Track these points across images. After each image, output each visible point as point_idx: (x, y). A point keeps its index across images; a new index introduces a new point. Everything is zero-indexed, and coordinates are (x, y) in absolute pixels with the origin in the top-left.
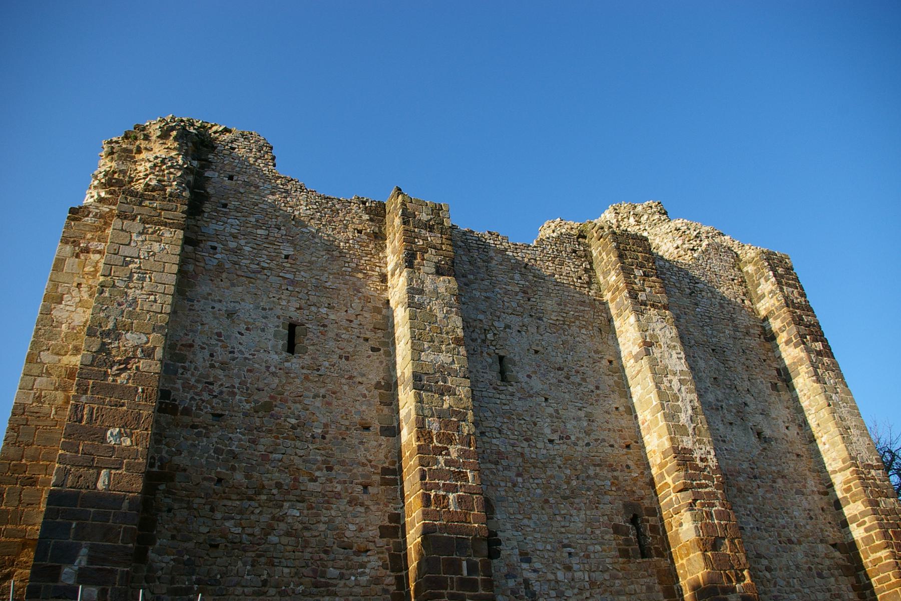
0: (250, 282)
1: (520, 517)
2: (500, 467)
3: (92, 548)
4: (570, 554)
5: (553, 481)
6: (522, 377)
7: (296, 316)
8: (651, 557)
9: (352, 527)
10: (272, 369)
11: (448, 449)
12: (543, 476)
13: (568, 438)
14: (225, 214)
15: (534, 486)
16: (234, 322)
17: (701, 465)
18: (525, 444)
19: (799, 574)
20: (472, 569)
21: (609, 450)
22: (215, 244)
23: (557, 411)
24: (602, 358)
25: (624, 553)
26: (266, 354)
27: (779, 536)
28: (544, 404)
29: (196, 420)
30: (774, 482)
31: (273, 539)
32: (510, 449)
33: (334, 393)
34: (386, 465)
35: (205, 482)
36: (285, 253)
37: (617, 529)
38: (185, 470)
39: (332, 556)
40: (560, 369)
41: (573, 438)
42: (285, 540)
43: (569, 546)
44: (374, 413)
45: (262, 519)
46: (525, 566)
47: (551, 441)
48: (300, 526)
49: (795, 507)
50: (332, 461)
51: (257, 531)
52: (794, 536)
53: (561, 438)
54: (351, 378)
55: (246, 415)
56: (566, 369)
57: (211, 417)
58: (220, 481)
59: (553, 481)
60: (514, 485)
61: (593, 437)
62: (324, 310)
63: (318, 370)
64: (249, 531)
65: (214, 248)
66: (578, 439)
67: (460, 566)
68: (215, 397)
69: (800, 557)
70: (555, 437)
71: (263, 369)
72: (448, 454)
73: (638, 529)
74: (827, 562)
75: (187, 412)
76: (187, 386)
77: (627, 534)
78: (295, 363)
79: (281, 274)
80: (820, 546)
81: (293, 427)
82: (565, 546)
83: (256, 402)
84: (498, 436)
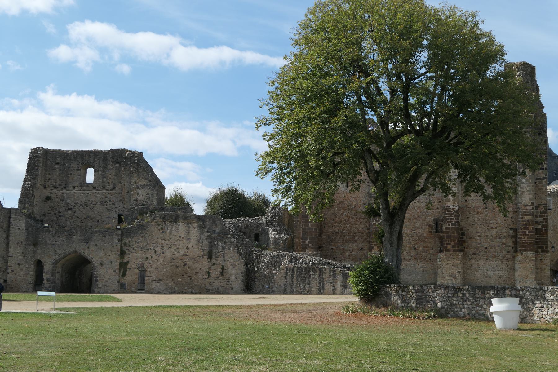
3: (310, 237)
9: (361, 228)
13: (420, 201)
17: (452, 210)
25: (431, 232)
31: (344, 232)
37: (430, 226)
41: (421, 201)
42: (347, 232)
44: (367, 200)
48: (349, 229)
51: (341, 230)
55: (338, 204)
74: (505, 234)
80: (504, 229)
81: (348, 206)
82: (413, 231)
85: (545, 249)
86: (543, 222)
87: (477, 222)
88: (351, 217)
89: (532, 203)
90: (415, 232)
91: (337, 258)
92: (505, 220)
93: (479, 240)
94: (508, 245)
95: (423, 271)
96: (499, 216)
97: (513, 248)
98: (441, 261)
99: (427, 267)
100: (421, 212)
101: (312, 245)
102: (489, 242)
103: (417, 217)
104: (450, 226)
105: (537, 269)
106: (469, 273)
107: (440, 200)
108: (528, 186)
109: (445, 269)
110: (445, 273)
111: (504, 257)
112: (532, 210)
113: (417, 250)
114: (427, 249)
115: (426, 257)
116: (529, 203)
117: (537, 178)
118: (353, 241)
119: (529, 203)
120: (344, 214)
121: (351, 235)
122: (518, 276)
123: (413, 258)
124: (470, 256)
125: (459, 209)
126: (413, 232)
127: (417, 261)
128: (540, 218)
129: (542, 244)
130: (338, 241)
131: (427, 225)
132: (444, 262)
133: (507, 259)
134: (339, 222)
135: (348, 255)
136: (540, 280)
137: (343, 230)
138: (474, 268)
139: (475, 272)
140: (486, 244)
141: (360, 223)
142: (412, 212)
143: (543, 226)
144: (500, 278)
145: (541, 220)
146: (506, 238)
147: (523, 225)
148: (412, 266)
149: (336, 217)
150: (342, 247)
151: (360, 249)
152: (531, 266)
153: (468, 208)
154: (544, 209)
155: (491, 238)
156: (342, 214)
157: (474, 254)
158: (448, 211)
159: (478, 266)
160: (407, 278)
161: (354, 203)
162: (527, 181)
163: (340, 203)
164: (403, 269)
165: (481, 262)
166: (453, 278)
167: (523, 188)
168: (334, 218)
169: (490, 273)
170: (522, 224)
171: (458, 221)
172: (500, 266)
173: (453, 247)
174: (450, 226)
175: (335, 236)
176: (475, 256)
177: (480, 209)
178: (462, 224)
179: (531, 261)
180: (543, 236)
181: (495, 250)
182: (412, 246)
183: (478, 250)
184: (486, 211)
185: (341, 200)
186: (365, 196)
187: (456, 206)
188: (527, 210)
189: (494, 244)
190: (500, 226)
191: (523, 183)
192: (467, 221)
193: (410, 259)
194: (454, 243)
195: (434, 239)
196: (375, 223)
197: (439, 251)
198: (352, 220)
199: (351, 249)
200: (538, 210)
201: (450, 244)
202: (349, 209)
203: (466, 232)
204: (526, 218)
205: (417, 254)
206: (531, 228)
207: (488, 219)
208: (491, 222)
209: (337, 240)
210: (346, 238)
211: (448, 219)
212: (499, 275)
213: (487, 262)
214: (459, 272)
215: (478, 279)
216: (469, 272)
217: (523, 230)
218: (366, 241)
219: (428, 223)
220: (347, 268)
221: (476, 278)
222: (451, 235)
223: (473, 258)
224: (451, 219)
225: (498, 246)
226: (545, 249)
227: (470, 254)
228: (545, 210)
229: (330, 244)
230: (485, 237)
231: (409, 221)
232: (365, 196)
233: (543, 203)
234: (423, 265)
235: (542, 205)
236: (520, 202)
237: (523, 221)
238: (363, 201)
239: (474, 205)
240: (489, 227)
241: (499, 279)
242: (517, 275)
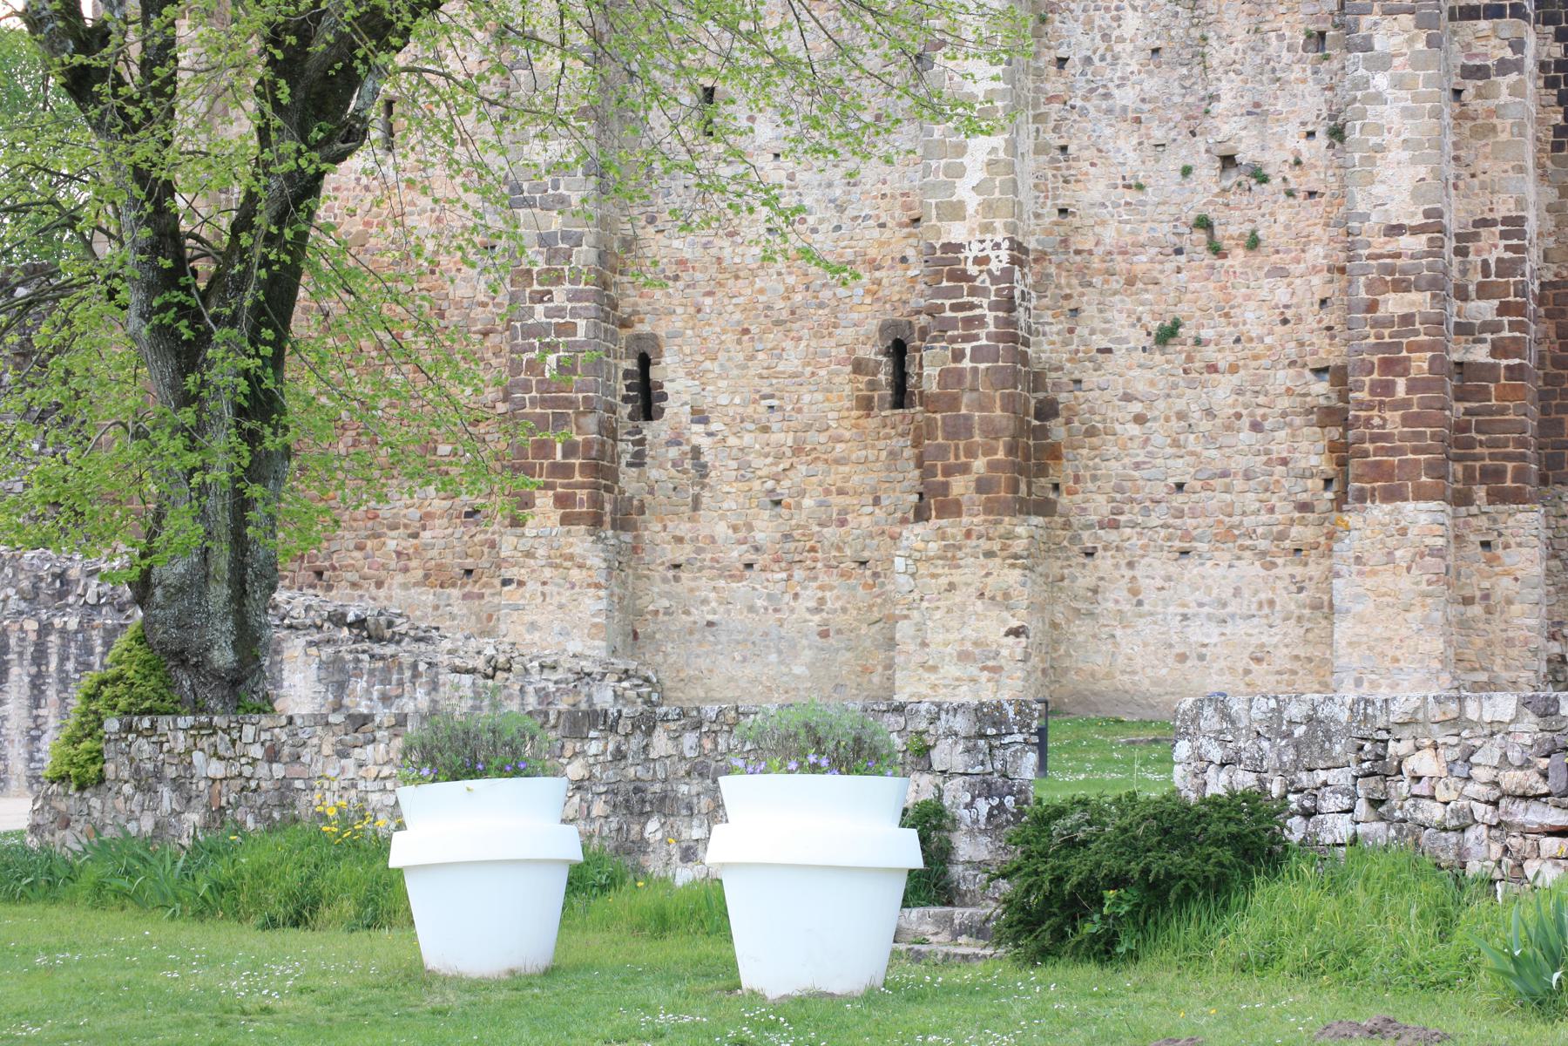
1: (700, 358)
4: (771, 407)
8: (912, 406)
11: (550, 292)
15: (730, 308)
17: (972, 269)
18: (726, 243)
20: (570, 449)
25: (866, 404)
32: (699, 251)
37: (859, 367)
43: (772, 396)
49: (1252, 305)
59: (762, 298)
60: (699, 311)
61: (850, 212)
66: (821, 221)
71: (353, 184)
72: (551, 300)
74: (1284, 403)
80: (1281, 374)
82: (764, 397)
85: (1509, 483)
86: (1495, 327)
87: (1125, 333)
89: (1427, 214)
90: (775, 402)
91: (334, 568)
92: (1285, 322)
93: (1137, 442)
94: (1303, 464)
95: (824, 634)
96: (1248, 298)
97: (1328, 482)
98: (912, 569)
99: (844, 610)
100: (807, 289)
102: (1192, 454)
103: (785, 315)
105: (1468, 601)
106: (1080, 638)
108: (1407, 113)
109: (938, 615)
110: (936, 638)
111: (1281, 537)
112: (1429, 254)
113: (784, 512)
115: (839, 549)
116: (1413, 214)
117: (1464, 67)
119: (1413, 214)
122: (1350, 644)
124: (1085, 535)
125: (1014, 261)
127: (790, 577)
128: (1483, 304)
129: (1493, 456)
132: (934, 576)
133: (1298, 551)
135: (399, 554)
136: (1484, 669)
138: (1110, 605)
139: (1118, 632)
142: (759, 284)
143: (1498, 349)
144: (1258, 660)
145: (1491, 316)
146: (1290, 425)
147: (1377, 347)
148: (759, 603)
151: (468, 515)
152: (1424, 586)
153: (1078, 252)
154: (1507, 248)
155: (1205, 425)
157: (1115, 525)
158: (952, 276)
159: (1134, 592)
160: (731, 679)
162: (1399, 83)
164: (710, 624)
165: (1154, 568)
166: (984, 668)
167: (1379, 130)
169: (1202, 632)
170: (1372, 340)
171: (1011, 336)
172: (1256, 593)
173: (982, 486)
174: (966, 363)
176: (1112, 536)
177: (1144, 258)
178: (1046, 349)
179: (1422, 556)
180: (1503, 411)
181: (1228, 497)
183: (1132, 500)
184: (1179, 271)
187: (997, 246)
188: (1398, 255)
189: (1219, 465)
190: (1256, 358)
191: (1378, 98)
192: (1071, 331)
193: (749, 566)
194: (992, 466)
195: (881, 444)
197: (911, 516)
199: (415, 513)
200: (1471, 257)
201: (965, 469)
203: (1063, 397)
204: (1394, 304)
205: (787, 537)
206: (1420, 363)
207: (1190, 318)
211: (953, 323)
212: (1254, 641)
213: (1184, 567)
214: (1016, 632)
215: (1134, 673)
216: (1081, 630)
217: (1375, 376)
219: (851, 351)
220: (350, 625)
221: (1121, 660)
222: (968, 418)
223: (1105, 549)
224: (968, 322)
225: (1248, 476)
226: (1509, 483)
227: (1090, 526)
228: (1509, 255)
230: (1175, 424)
231: (739, 342)
233: (1498, 216)
234: (822, 601)
235: (1493, 223)
236: (1361, 208)
237: (1376, 324)
239: (1109, 235)
240: (1197, 365)
241: (1254, 666)
242: (1344, 643)
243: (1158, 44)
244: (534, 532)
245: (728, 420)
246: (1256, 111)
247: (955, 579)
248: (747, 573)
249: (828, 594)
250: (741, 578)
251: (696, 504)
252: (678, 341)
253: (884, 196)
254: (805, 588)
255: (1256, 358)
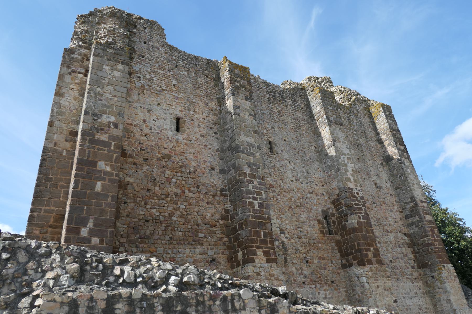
0: (157, 96)
1: (280, 214)
2: (270, 191)
3: (95, 219)
5: (293, 199)
6: (280, 152)
7: (180, 115)
8: (333, 234)
9: (209, 215)
10: (170, 139)
11: (253, 181)
12: (289, 196)
13: (299, 180)
14: (143, 61)
16: (151, 114)
17: (357, 196)
18: (281, 182)
19: (391, 246)
21: (315, 186)
22: (140, 75)
23: (294, 168)
24: (312, 145)
25: (322, 232)
26: (167, 131)
27: (383, 229)
28: (288, 164)
29: (135, 161)
30: (381, 205)
31: (174, 218)
32: (275, 183)
33: (198, 152)
34: (222, 187)
35: (141, 191)
36: (173, 83)
37: (319, 222)
38: (132, 184)
39: (200, 227)
40: (295, 149)
41: (301, 180)
42: (179, 219)
44: (216, 163)
45: (169, 209)
46: (282, 235)
47: (292, 181)
48: (185, 213)
50: (200, 184)
51: (167, 214)
52: (390, 229)
53: (296, 180)
54: (205, 146)
55: (159, 160)
56: (297, 149)
57: (142, 160)
58: (148, 190)
59: (293, 199)
60: (277, 199)
62: (192, 113)
63: (191, 141)
64: (163, 214)
65: (140, 77)
66: (303, 181)
67: (260, 233)
68: (144, 150)
69: (392, 238)
70: (293, 179)
71: (166, 139)
72: (253, 183)
73: (327, 222)
74: (402, 241)
75: (131, 156)
76: (130, 144)
77: (323, 224)
78: (180, 137)
79: (172, 94)
81: (181, 167)
83: (162, 153)
84: (270, 177)
88: (189, 190)
90: (301, 230)
92: (396, 222)
101: (101, 241)
104: (362, 220)
107: (323, 183)
114: (323, 261)
115: (326, 277)
118: (193, 243)
120: (174, 180)
121: (190, 227)
123: (308, 280)
126: (299, 229)
127: (316, 286)
130: (159, 239)
131: (315, 220)
132: (373, 283)
134: (163, 196)
137: (171, 215)
140: (389, 255)
141: (208, 203)
149: (155, 185)
150: (169, 256)
151: (211, 261)
156: (169, 181)
161: (194, 164)
163: (163, 158)
168: (150, 186)
175: (152, 228)
182: (301, 255)
185: (166, 152)
186: (212, 155)
188: (424, 207)
193: (304, 283)
196: (251, 200)
198: (191, 195)
201: (369, 250)
202: (182, 172)
205: (312, 272)
208: (385, 223)
209: (156, 237)
210: (177, 233)
212: (418, 304)
218: (221, 243)
229: (137, 247)
232: (212, 155)
238: (210, 162)
243: (358, 157)
244: (259, 265)
245: (290, 234)
246: (377, 175)
247: (378, 284)
248: (303, 285)
249: (327, 292)
250: (302, 287)
251: (286, 261)
252: (273, 207)
253: (316, 178)
254: (321, 290)
255: (394, 230)
